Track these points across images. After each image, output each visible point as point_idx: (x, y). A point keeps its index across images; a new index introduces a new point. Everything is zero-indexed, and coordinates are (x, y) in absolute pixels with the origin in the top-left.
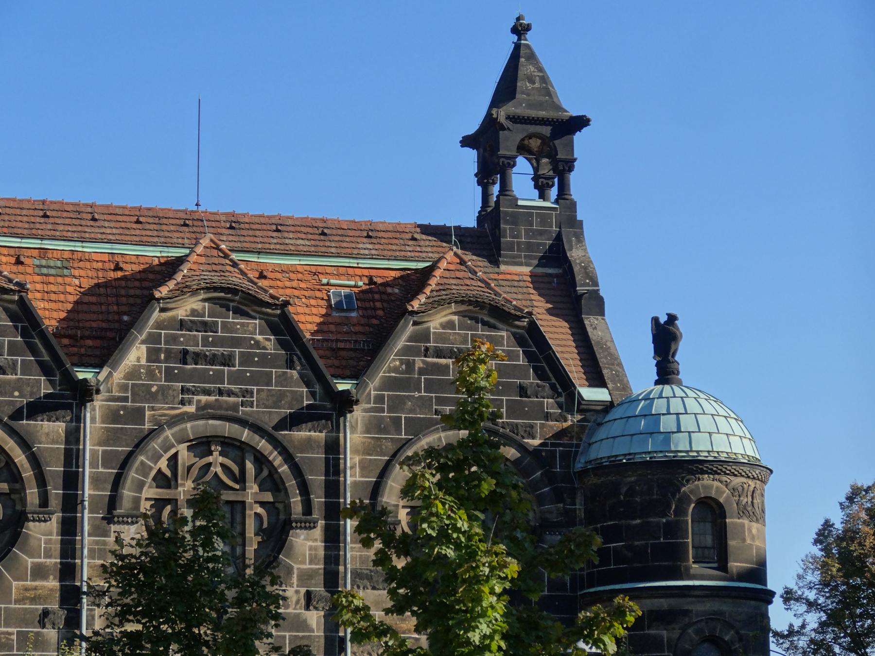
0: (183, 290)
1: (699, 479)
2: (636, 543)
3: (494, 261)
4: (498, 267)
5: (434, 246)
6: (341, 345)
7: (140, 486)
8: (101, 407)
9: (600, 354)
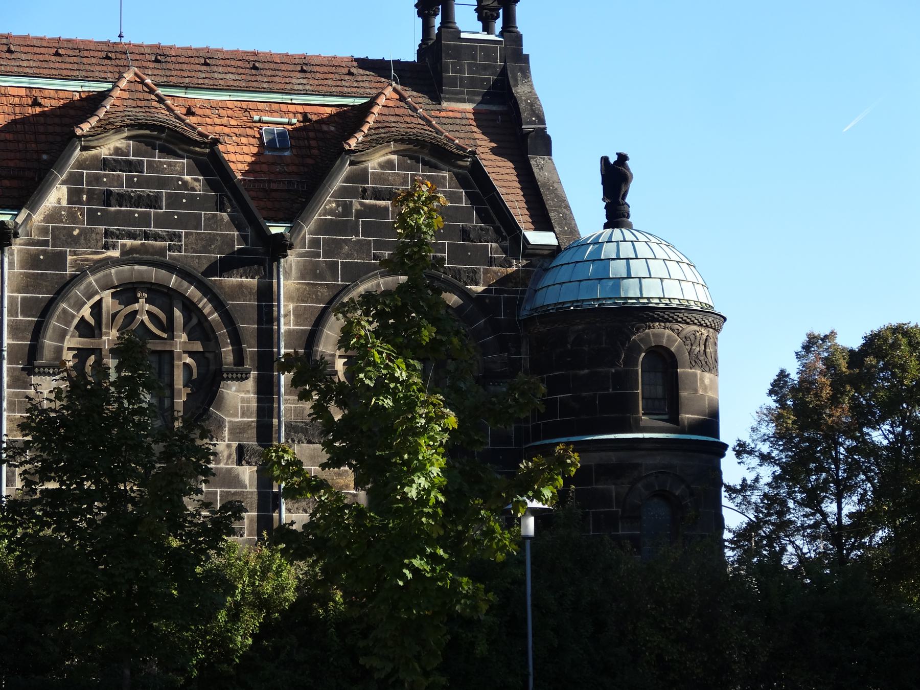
0: (105, 128)
1: (650, 328)
2: (584, 394)
3: (436, 98)
4: (440, 104)
5: (372, 81)
6: (274, 186)
7: (62, 335)
8: (20, 251)
9: (546, 195)
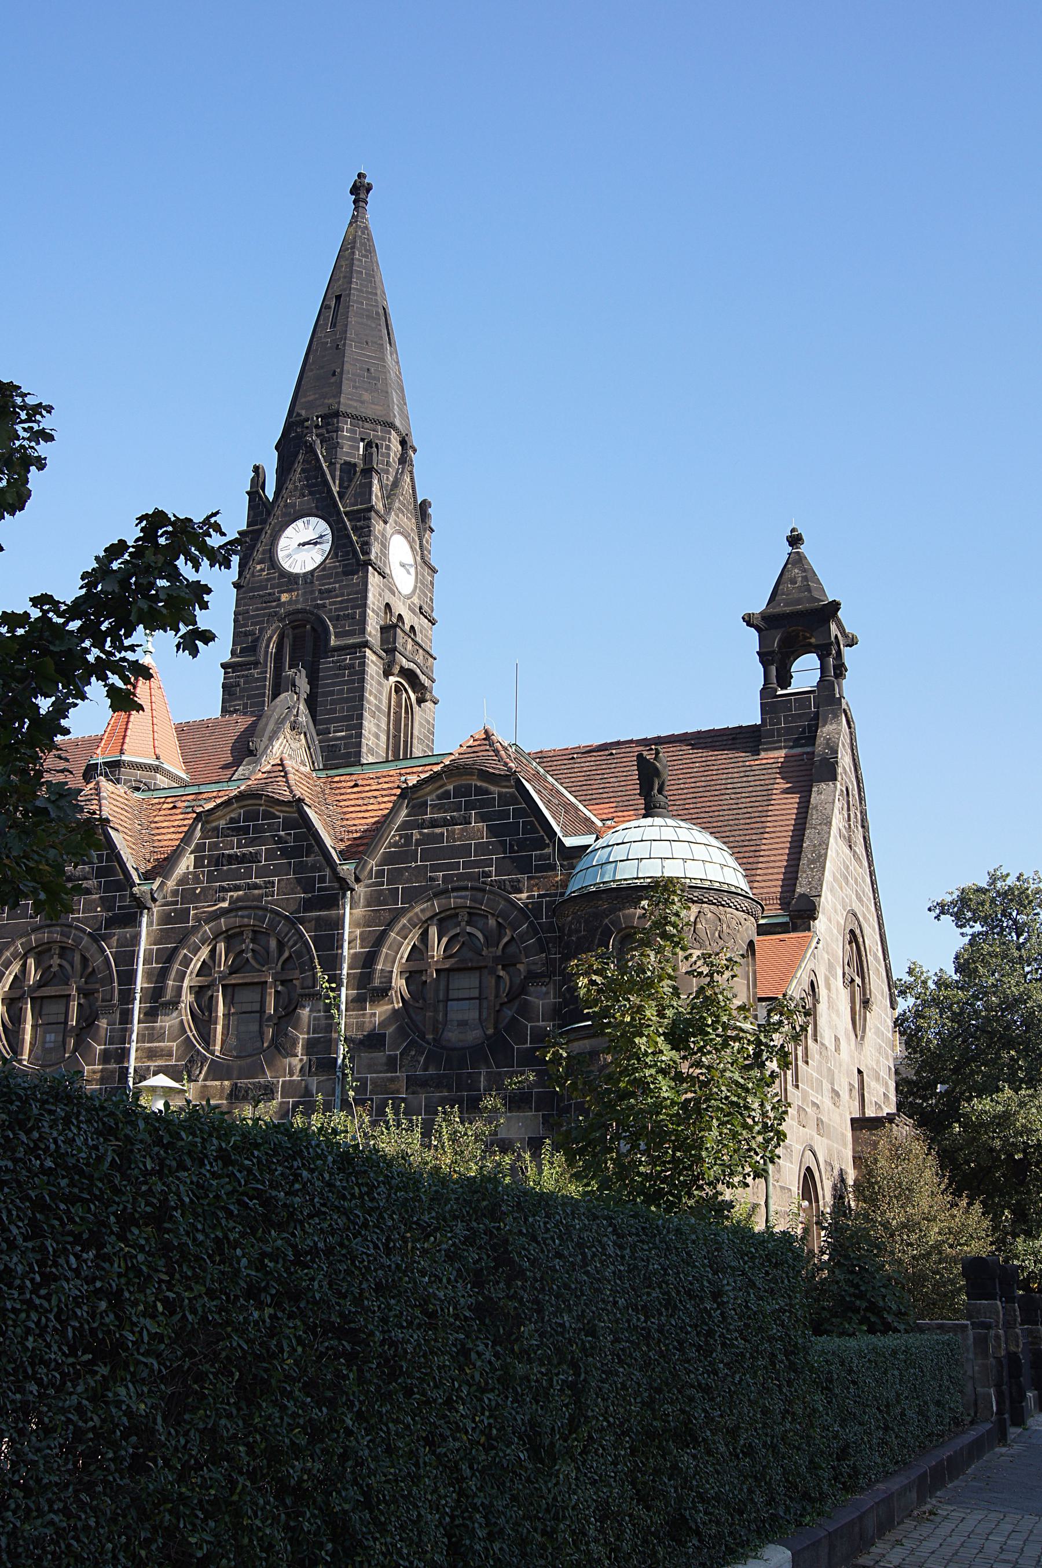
7: (181, 976)
